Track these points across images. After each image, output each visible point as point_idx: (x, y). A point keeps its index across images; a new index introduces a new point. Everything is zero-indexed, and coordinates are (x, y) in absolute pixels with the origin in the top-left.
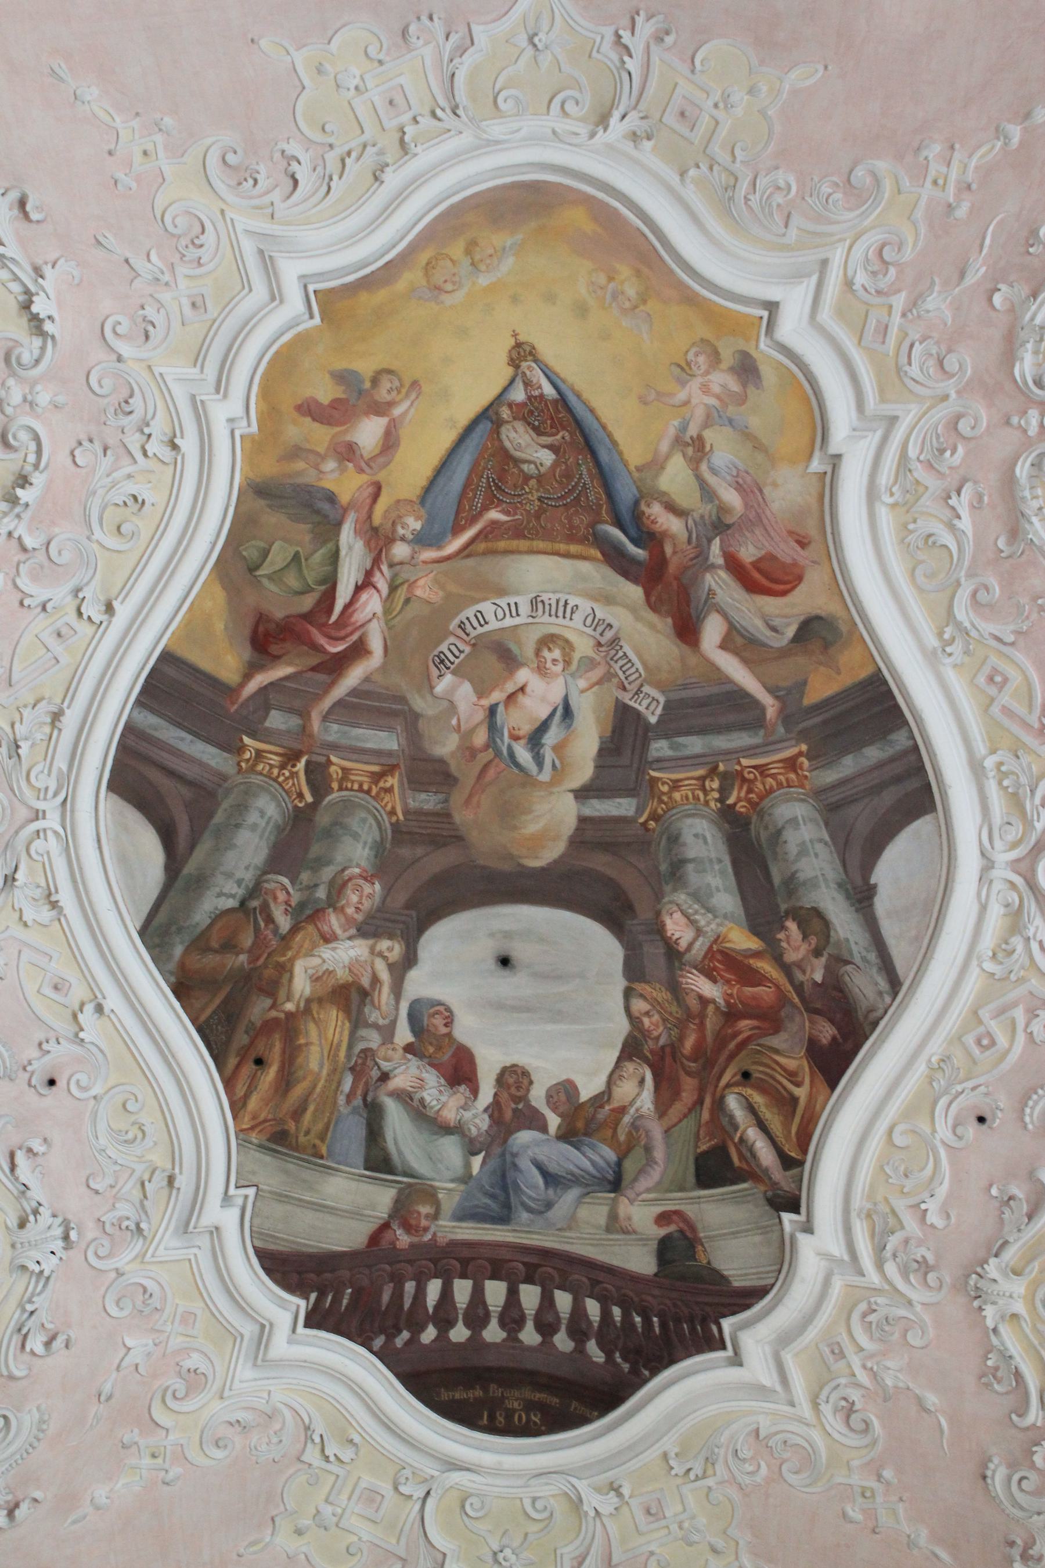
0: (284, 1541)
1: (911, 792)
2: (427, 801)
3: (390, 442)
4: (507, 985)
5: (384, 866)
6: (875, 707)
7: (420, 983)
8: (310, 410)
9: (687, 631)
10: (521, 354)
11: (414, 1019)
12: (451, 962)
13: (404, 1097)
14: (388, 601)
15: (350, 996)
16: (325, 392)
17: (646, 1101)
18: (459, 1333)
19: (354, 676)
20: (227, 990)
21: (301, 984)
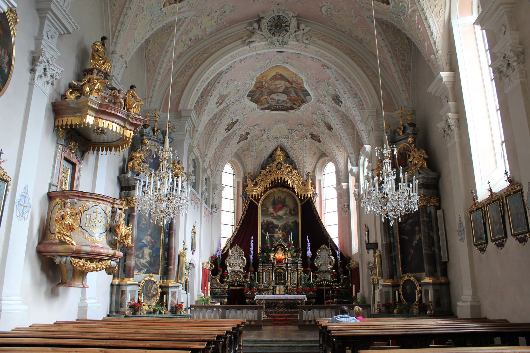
1: (309, 95)
9: (291, 84)
12: (273, 96)
15: (266, 99)
20: (257, 101)
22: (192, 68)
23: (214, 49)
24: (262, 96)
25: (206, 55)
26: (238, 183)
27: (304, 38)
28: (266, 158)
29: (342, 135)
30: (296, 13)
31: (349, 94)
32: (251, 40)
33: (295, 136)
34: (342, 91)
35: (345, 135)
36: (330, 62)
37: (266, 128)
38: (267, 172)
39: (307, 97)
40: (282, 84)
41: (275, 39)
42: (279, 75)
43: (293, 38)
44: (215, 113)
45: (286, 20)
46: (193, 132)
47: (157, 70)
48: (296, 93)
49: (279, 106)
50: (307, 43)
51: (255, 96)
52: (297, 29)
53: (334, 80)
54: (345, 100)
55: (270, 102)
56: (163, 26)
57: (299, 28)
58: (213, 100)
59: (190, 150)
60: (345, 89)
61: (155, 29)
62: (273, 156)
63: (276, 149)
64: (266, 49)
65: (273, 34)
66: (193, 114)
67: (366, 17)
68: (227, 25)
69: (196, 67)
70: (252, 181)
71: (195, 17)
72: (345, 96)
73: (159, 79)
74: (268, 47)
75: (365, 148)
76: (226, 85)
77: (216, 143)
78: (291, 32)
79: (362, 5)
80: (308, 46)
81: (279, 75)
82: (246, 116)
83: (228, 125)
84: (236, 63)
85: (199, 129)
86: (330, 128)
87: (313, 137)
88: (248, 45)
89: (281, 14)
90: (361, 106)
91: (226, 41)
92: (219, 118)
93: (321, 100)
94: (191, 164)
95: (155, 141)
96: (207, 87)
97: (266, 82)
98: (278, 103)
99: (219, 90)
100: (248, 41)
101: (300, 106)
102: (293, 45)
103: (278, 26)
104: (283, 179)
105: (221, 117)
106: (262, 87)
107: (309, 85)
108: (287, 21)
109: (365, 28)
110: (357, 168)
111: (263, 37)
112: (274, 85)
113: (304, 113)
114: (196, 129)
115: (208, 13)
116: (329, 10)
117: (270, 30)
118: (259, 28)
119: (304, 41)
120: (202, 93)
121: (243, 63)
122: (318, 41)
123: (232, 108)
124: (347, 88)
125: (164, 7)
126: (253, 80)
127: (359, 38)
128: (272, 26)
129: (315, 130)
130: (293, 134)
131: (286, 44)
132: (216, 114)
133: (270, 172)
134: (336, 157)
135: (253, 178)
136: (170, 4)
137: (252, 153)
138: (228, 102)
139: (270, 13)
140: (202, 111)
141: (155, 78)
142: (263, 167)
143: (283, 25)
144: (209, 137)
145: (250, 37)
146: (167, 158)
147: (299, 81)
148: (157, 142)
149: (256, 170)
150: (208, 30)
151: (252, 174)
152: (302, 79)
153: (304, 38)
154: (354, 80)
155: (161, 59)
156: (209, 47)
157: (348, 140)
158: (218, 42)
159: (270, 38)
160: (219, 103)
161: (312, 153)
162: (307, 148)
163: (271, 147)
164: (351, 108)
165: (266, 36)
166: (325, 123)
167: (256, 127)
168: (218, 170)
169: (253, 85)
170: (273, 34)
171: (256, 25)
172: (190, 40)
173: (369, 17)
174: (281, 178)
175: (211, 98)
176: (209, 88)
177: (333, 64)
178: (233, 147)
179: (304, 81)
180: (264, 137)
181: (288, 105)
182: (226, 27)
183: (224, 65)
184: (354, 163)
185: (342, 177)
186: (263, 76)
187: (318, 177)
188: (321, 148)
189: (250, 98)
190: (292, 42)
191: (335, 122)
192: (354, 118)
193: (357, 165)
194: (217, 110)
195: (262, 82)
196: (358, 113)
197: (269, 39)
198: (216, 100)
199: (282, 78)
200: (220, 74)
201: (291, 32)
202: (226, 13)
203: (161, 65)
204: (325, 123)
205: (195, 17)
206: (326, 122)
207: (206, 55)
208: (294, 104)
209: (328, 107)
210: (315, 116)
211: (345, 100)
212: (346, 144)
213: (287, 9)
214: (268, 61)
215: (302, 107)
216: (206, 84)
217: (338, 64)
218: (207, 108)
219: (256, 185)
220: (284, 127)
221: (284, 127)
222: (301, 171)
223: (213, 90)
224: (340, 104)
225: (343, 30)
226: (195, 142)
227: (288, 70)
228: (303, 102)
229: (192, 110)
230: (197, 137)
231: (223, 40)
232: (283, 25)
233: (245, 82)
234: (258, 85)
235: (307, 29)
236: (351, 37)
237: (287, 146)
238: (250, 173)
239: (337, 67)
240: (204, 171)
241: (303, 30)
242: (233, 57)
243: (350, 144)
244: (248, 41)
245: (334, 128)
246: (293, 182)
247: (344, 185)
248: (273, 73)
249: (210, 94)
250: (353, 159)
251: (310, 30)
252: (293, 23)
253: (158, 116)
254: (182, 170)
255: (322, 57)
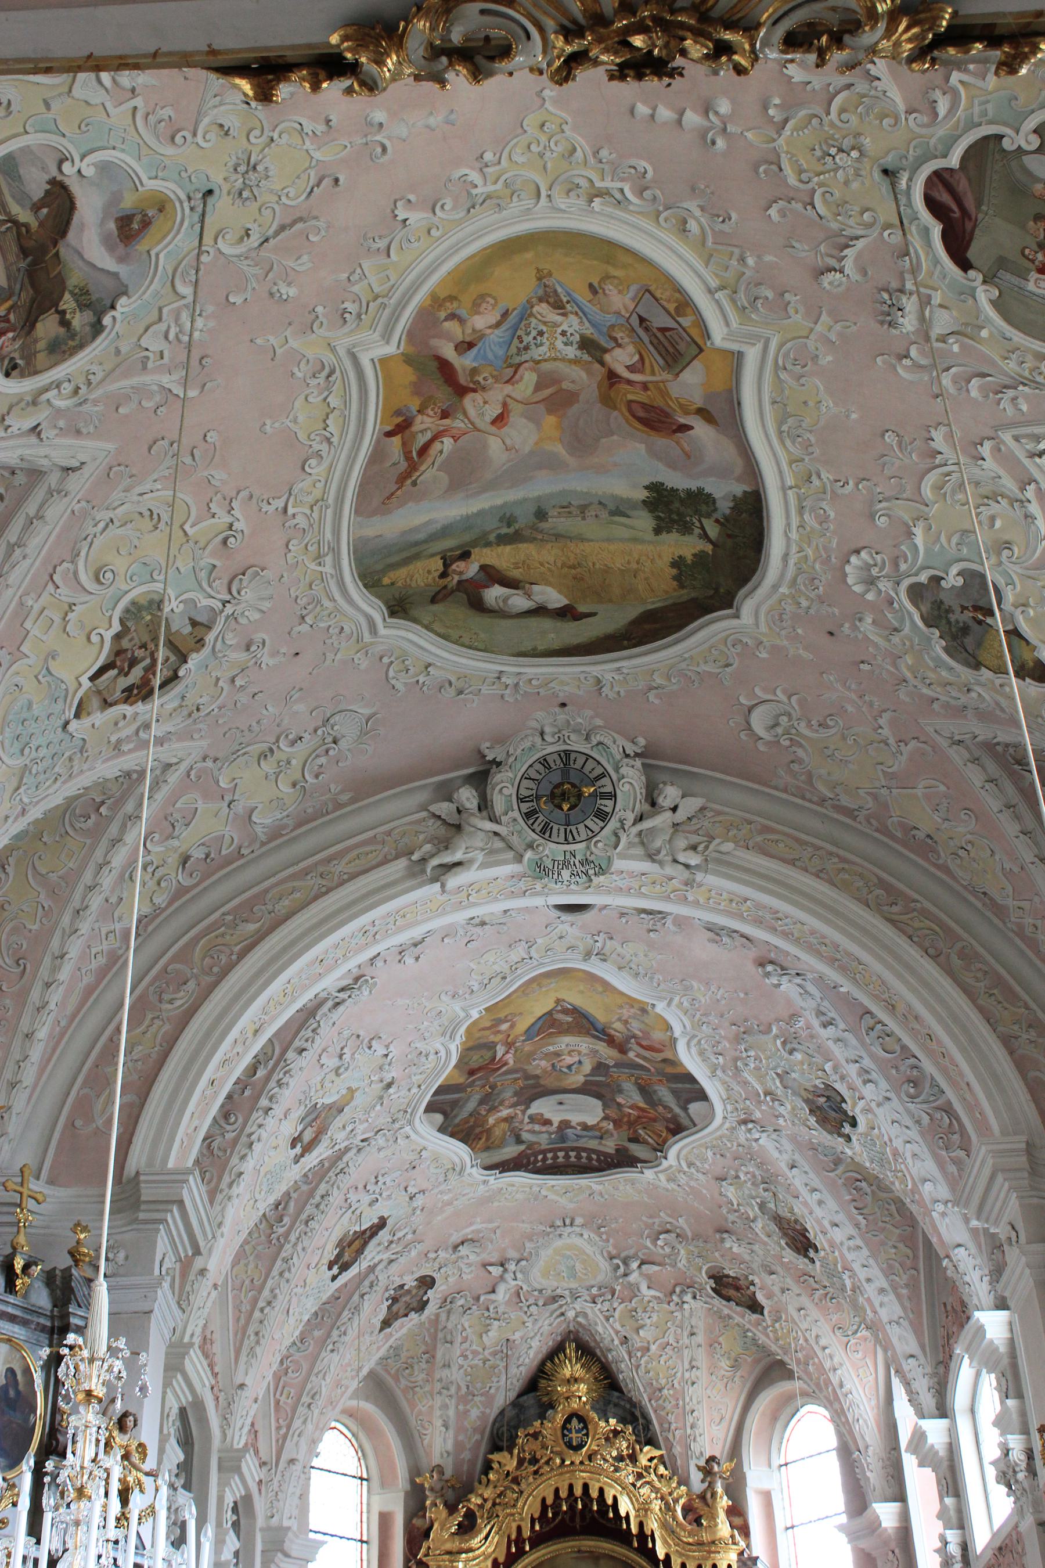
0: (496, 1204)
2: (531, 1082)
3: (512, 1027)
4: (561, 1107)
5: (516, 1094)
6: (690, 1078)
7: (530, 1112)
8: (483, 1029)
9: (623, 1050)
10: (558, 1001)
11: (530, 1117)
12: (542, 1107)
13: (528, 1131)
14: (514, 1055)
15: (508, 1119)
16: (488, 1024)
17: (611, 1126)
18: (550, 1161)
19: (504, 1069)
20: (468, 1133)
21: (491, 1121)
22: (191, 985)
23: (287, 902)
24: (493, 1109)
25: (252, 927)
26: (385, 1520)
27: (681, 843)
28: (512, 1395)
29: (862, 1274)
30: (642, 741)
31: (884, 1084)
32: (447, 858)
33: (644, 1287)
34: (852, 1070)
35: (875, 1272)
36: (797, 942)
37: (512, 1254)
38: (521, 1462)
39: (694, 1108)
40: (578, 1052)
41: (553, 850)
42: (565, 1011)
43: (630, 845)
44: (284, 1188)
45: (599, 771)
46: (184, 1275)
47: (35, 995)
48: (644, 1090)
49: (567, 1150)
50: (693, 862)
51: (457, 1111)
52: (647, 807)
53: (815, 1023)
54: (867, 1110)
55: (525, 1136)
56: (70, 801)
57: (653, 804)
58: (276, 1129)
59: (174, 1366)
60: (867, 1062)
61: (35, 813)
62: (543, 1383)
63: (556, 1352)
64: (513, 895)
65: (545, 831)
66: (194, 1191)
67: (944, 743)
68: (345, 798)
69: (210, 979)
70: (452, 1509)
71: (209, 764)
72: (868, 1091)
73: (42, 1034)
74: (522, 885)
75: (981, 1330)
76: (330, 1062)
77: (283, 1329)
78: (621, 821)
79: (925, 691)
80: (699, 877)
81: (565, 1011)
82: (419, 1201)
83: (343, 1245)
84: (379, 963)
85: (212, 1266)
86: (801, 1242)
87: (728, 1287)
88: (434, 880)
89: (577, 744)
90: (946, 1131)
91: (340, 867)
92: (300, 1211)
93: (758, 1115)
94: (172, 1429)
95: (12, 1319)
96: (253, 1069)
97: (509, 1045)
98: (563, 1139)
99: (304, 1082)
100: (435, 862)
101: (660, 1148)
102: (631, 874)
103: (564, 796)
104: (594, 1494)
105: (309, 1210)
106: (492, 1066)
107: (702, 1053)
108: (602, 776)
109: (942, 788)
110: (943, 1423)
111: (499, 844)
112: (547, 1056)
113: (683, 1179)
114: (199, 1263)
115: (264, 746)
116: (784, 720)
117: (528, 815)
118: (485, 805)
119: (681, 858)
120: (229, 1097)
121: (409, 960)
122: (741, 853)
123: (360, 1166)
124: (872, 1056)
125: (77, 716)
126: (452, 1037)
127: (920, 835)
128: (538, 798)
129: (735, 1255)
130: (633, 1277)
131: (602, 871)
132: (287, 1195)
133: (534, 1461)
134: (835, 1381)
135: (456, 1492)
136: (106, 704)
137: (446, 1372)
138: (340, 1136)
139: (527, 744)
140: (226, 1179)
141: (24, 1026)
142: (501, 1437)
143: (588, 790)
144: (255, 1300)
145: (444, 844)
146: (100, 1391)
147: (658, 1036)
148: (25, 1323)
149: (466, 1455)
150: (263, 820)
151: (448, 1473)
152: (669, 1028)
153: (681, 843)
154: (910, 1018)
155: (55, 943)
156: (266, 891)
157: (892, 1297)
158: (306, 872)
159: (530, 846)
160: (302, 1145)
161: (724, 1364)
162: (700, 1338)
163: (535, 1343)
164: (898, 1143)
165: (515, 840)
166: (778, 1219)
167: (463, 1250)
168: (292, 1461)
169: (454, 1061)
170: (543, 831)
171: (467, 796)
172: (185, 860)
173: (960, 742)
174: (586, 1487)
175: (270, 1122)
176: (261, 1073)
177: (810, 949)
178: (363, 1345)
179: (677, 1031)
180: (502, 1294)
181: (609, 1146)
182: (339, 806)
183: (330, 970)
184: (928, 1401)
185: (874, 1476)
186: (497, 1015)
187: (757, 1477)
188: (762, 1339)
189: (439, 1118)
190: (629, 865)
191: (824, 1214)
192: (915, 1190)
193: (943, 1410)
194: (295, 1173)
195: (491, 1046)
196: (928, 1166)
197: (529, 855)
198: (290, 1128)
199: (582, 1023)
200: (309, 1014)
201: (621, 821)
202: (343, 744)
203: (55, 969)
204: (778, 1219)
205: (209, 764)
206: (785, 1213)
207: (252, 927)
208: (635, 1139)
209: (787, 1146)
210: (731, 1192)
211: (867, 1110)
212: (884, 1314)
213: (599, 722)
214: (520, 951)
215: (672, 1153)
216: (247, 1060)
217: (836, 946)
218: (249, 1166)
219: (468, 1527)
220: (589, 1249)
221: (589, 1249)
222: (677, 1450)
223: (280, 1084)
224: (847, 1129)
225: (845, 801)
226: (195, 1328)
227: (606, 985)
228: (677, 1129)
229: (189, 1172)
230: (205, 1297)
231: (329, 860)
232: (588, 790)
233: (421, 1045)
234: (476, 1059)
235: (689, 806)
236: (885, 831)
237: (606, 1331)
238: (440, 1469)
239: (832, 961)
240: (231, 1465)
241: (674, 809)
242: (372, 935)
243: (898, 1311)
244: (435, 862)
245: (820, 1241)
246: (644, 1508)
247: (886, 1513)
248: (541, 1005)
249: (264, 1102)
250: (922, 1385)
251: (703, 809)
252: (630, 782)
253: (31, 1204)
254: (135, 1458)
255: (758, 922)
